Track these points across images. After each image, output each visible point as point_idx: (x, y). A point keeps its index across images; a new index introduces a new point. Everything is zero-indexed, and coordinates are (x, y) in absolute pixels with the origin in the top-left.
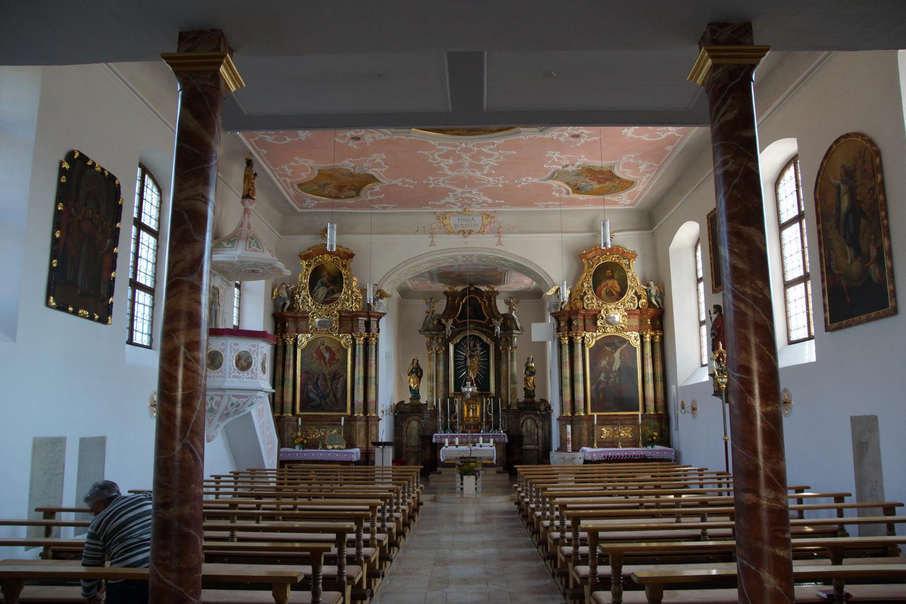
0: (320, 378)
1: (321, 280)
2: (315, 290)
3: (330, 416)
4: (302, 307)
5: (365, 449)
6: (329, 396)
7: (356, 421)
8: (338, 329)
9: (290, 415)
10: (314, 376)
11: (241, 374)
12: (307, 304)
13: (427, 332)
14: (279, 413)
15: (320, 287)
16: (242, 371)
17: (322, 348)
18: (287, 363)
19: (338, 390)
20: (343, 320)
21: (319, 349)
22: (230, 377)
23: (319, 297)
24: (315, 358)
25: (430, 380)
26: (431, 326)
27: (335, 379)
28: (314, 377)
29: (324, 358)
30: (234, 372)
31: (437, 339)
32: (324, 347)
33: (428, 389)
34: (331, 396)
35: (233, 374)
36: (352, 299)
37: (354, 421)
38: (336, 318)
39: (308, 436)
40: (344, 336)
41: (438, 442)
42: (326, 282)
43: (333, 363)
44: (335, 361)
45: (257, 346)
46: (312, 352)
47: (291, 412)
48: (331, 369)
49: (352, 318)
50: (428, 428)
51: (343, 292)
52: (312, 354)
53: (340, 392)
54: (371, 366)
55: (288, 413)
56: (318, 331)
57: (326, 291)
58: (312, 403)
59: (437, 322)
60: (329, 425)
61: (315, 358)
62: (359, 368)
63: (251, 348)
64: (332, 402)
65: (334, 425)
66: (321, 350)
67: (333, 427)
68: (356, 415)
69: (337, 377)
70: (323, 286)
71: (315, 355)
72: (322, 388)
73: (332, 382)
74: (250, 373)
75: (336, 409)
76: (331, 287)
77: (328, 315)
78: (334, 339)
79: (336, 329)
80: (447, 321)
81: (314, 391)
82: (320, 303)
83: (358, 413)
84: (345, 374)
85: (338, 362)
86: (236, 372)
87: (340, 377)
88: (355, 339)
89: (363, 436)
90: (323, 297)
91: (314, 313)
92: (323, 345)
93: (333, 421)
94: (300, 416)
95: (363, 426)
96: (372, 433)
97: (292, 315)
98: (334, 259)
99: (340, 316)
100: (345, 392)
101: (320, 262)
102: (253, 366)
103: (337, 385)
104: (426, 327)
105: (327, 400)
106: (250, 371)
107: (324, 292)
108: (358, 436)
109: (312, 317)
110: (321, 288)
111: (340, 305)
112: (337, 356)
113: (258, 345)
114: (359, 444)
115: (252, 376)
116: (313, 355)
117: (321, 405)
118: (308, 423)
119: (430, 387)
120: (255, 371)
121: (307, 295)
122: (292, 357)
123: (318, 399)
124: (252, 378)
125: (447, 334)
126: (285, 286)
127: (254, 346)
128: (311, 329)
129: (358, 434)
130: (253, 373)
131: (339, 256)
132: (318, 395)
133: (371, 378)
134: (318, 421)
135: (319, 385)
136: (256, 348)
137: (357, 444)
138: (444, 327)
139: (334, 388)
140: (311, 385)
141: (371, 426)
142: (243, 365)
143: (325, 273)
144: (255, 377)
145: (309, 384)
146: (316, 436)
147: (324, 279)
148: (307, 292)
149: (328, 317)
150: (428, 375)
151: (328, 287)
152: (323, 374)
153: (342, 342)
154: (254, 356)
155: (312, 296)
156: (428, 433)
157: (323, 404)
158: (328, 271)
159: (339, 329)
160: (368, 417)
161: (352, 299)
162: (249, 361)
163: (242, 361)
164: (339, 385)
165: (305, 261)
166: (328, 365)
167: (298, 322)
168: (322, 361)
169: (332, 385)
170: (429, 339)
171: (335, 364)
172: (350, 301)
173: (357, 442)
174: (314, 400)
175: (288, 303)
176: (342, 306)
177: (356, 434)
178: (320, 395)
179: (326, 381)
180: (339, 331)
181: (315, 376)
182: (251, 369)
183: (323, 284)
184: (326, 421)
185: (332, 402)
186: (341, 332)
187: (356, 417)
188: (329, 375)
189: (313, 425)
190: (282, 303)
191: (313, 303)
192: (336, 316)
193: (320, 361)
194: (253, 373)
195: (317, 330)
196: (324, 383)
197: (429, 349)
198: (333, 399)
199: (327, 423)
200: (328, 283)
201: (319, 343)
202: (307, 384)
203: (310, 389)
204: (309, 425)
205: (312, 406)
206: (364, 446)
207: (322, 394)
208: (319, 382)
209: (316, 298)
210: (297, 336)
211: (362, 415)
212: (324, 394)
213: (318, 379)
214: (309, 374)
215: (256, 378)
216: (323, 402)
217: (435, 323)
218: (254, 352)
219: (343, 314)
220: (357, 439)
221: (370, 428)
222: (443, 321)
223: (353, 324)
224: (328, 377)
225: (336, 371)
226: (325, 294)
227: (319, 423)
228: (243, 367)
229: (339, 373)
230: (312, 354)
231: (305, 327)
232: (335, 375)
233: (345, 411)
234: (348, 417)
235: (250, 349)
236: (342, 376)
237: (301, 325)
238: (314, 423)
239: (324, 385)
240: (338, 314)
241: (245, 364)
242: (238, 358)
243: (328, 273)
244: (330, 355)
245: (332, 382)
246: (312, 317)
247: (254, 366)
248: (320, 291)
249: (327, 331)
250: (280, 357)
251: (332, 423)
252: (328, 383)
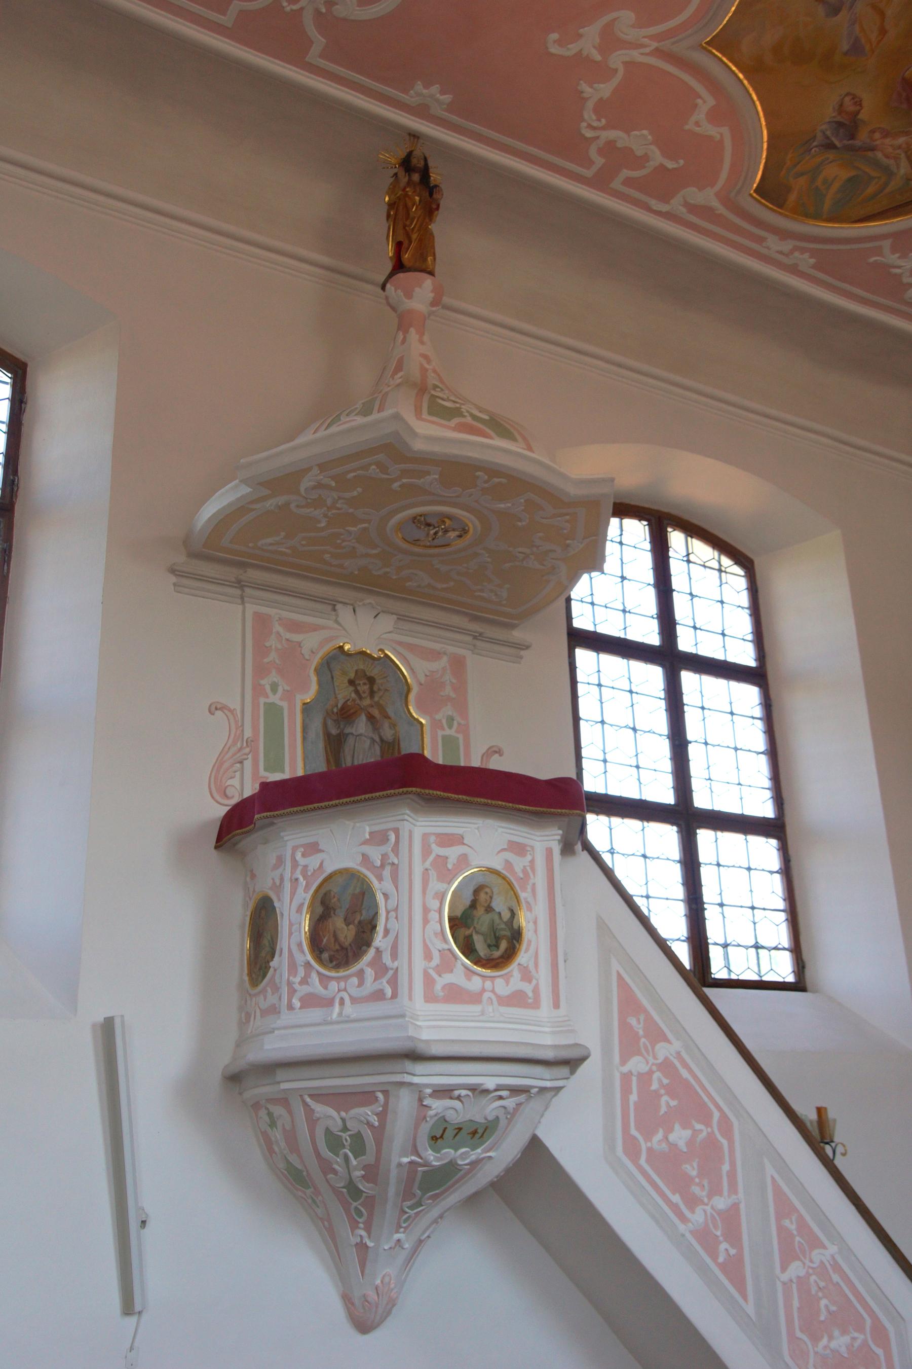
11: (333, 986)
16: (337, 967)
22: (290, 1007)
30: (304, 981)
35: (303, 990)
45: (392, 837)
63: (367, 849)
74: (369, 973)
86: (315, 977)
102: (379, 940)
106: (371, 964)
113: (396, 831)
115: (377, 986)
120: (387, 959)
124: (378, 996)
127: (379, 838)
130: (381, 969)
136: (387, 848)
142: (341, 938)
144: (389, 992)
154: (380, 887)
162: (365, 915)
163: (338, 922)
182: (371, 953)
194: (381, 969)
215: (394, 996)
218: (383, 866)
228: (342, 948)
235: (365, 858)
241: (347, 934)
242: (320, 910)
247: (387, 932)
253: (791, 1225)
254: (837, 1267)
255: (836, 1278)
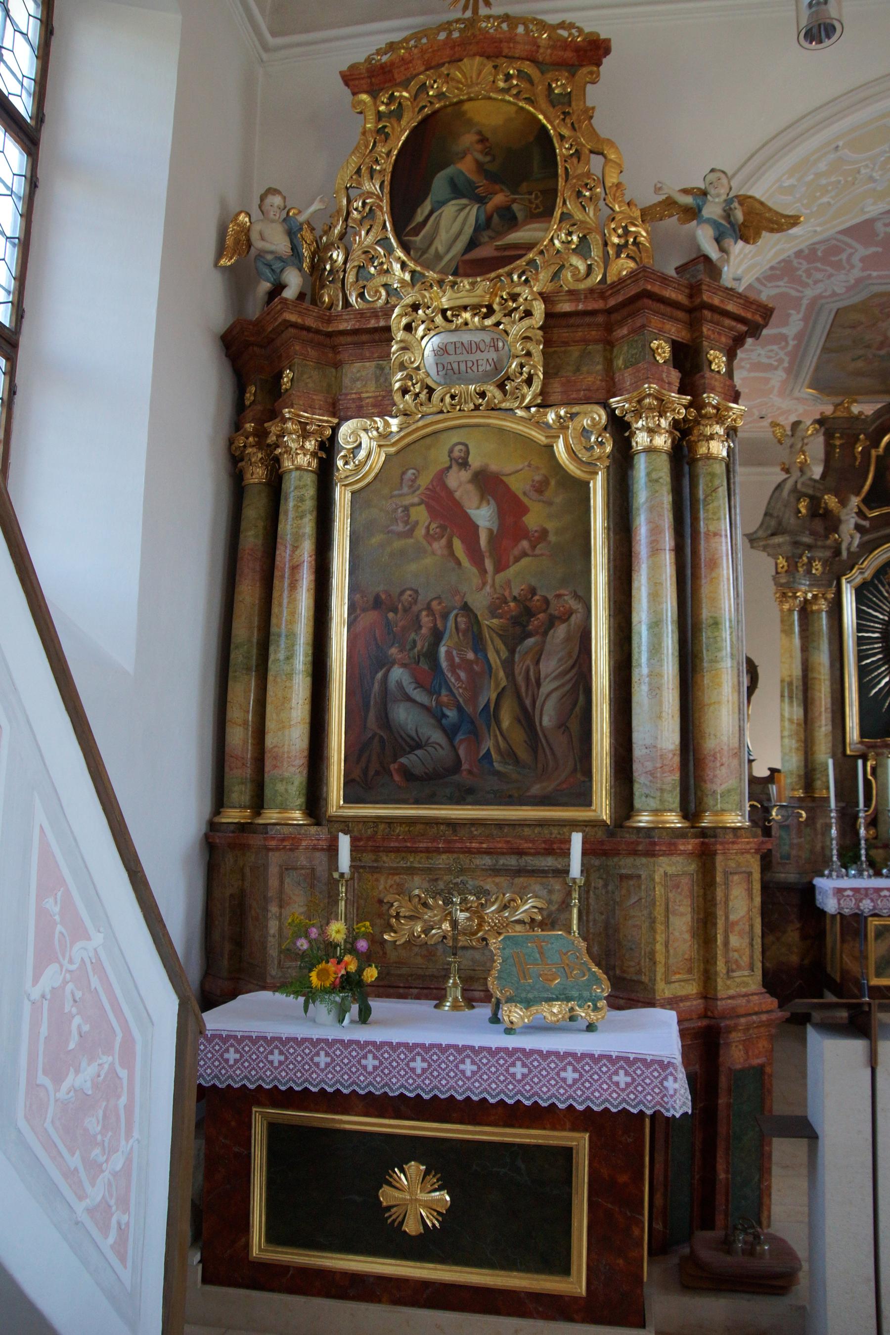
0: (451, 623)
1: (449, 171)
2: (419, 217)
3: (500, 825)
4: (361, 295)
5: (698, 1003)
6: (498, 723)
7: (650, 853)
8: (537, 385)
9: (297, 816)
10: (418, 616)
12: (384, 279)
13: (778, 540)
14: (244, 807)
15: (443, 203)
17: (457, 480)
18: (284, 555)
19: (546, 688)
20: (566, 344)
21: (445, 486)
23: (439, 245)
24: (420, 532)
25: (791, 697)
26: (790, 520)
27: (529, 635)
28: (417, 625)
29: (469, 530)
31: (811, 560)
32: (465, 475)
33: (782, 730)
34: (506, 722)
36: (606, 244)
37: (635, 853)
38: (527, 322)
39: (391, 929)
40: (573, 416)
41: (846, 911)
42: (473, 177)
43: (516, 552)
44: (525, 544)
46: (407, 501)
47: (300, 801)
48: (508, 583)
49: (609, 328)
50: (788, 857)
51: (557, 214)
52: (406, 509)
53: (555, 696)
54: (714, 564)
55: (284, 807)
56: (436, 396)
57: (472, 220)
58: (403, 760)
59: (808, 508)
60: (495, 871)
61: (420, 532)
62: (654, 569)
64: (510, 756)
65: (519, 872)
66: (450, 493)
67: (519, 881)
68: (644, 820)
69: (534, 623)
70: (463, 196)
71: (420, 514)
72: (457, 681)
73: (512, 652)
75: (536, 789)
76: (499, 199)
77: (491, 311)
78: (518, 436)
79: (529, 382)
80: (843, 503)
81: (419, 696)
82: (442, 272)
83: (656, 812)
84: (573, 604)
85: (541, 548)
87: (552, 622)
88: (628, 426)
89: (687, 936)
90: (460, 245)
91: (415, 307)
92: (464, 464)
93: (520, 853)
94: (345, 824)
95: (685, 881)
96: (733, 917)
97: (310, 322)
98: (508, 77)
99: (548, 315)
100: (581, 698)
101: (440, 96)
103: (537, 662)
104: (773, 523)
105: (488, 744)
107: (464, 223)
108: (660, 938)
109: (408, 328)
110: (449, 210)
111: (544, 275)
112: (533, 520)
114: (668, 982)
116: (413, 518)
117: (456, 766)
118: (388, 860)
119: (791, 721)
121: (383, 242)
122: (308, 526)
123: (437, 736)
125: (844, 546)
126: (277, 200)
128: (405, 391)
129: (660, 927)
131: (533, 61)
132: (438, 717)
133: (716, 624)
134: (438, 851)
135: (444, 664)
137: (660, 985)
138: (831, 523)
139: (520, 680)
140: (404, 666)
141: (726, 884)
143: (468, 139)
145: (393, 664)
146: (426, 931)
147: (466, 167)
148: (384, 226)
149: (488, 322)
150: (782, 681)
151: (481, 200)
152: (466, 608)
153: (560, 448)
155: (406, 248)
156: (788, 875)
157: (465, 766)
158: (480, 133)
159: (544, 385)
160: (704, 833)
161: (606, 244)
164: (550, 666)
165: (374, 95)
166: (489, 564)
167: (337, 365)
168: (458, 545)
169: (508, 665)
170: (782, 561)
171: (525, 554)
172: (596, 252)
173: (660, 970)
174: (417, 744)
175: (294, 282)
176: (556, 276)
177: (652, 929)
178: (451, 714)
179: (478, 643)
180: (543, 393)
181: (425, 619)
183: (458, 190)
184: (480, 852)
185: (510, 756)
186: (554, 398)
187: (648, 831)
188: (493, 615)
189: (411, 871)
190: (265, 286)
191: (413, 273)
192: (528, 314)
193: (450, 545)
195: (431, 391)
196: (471, 656)
197: (784, 595)
198: (518, 737)
199: (487, 861)
200: (481, 182)
201: (440, 457)
202: (383, 663)
203: (400, 685)
204: (395, 871)
205: (408, 775)
206: (692, 989)
207: (460, 709)
208: (443, 650)
209: (425, 251)
210: (335, 429)
211: (674, 820)
212: (469, 709)
213: (437, 636)
214: (395, 610)
216: (462, 752)
217: (803, 511)
219: (566, 307)
220: (660, 957)
221: (720, 893)
222: (831, 501)
223: (609, 363)
224: (489, 622)
225: (533, 591)
226: (469, 231)
227: (442, 860)
229: (546, 601)
230: (406, 509)
231: (372, 386)
232: (528, 613)
233: (584, 798)
234: (600, 834)
236: (566, 616)
237: (354, 381)
238: (415, 861)
239: (467, 665)
240: (539, 308)
243: (483, 140)
244: (501, 513)
245: (512, 652)
246: (408, 328)
248: (443, 223)
249: (482, 395)
250: (252, 539)
251: (512, 861)
252: (492, 656)
253: (53, 907)
254: (98, 966)
255: (95, 982)
